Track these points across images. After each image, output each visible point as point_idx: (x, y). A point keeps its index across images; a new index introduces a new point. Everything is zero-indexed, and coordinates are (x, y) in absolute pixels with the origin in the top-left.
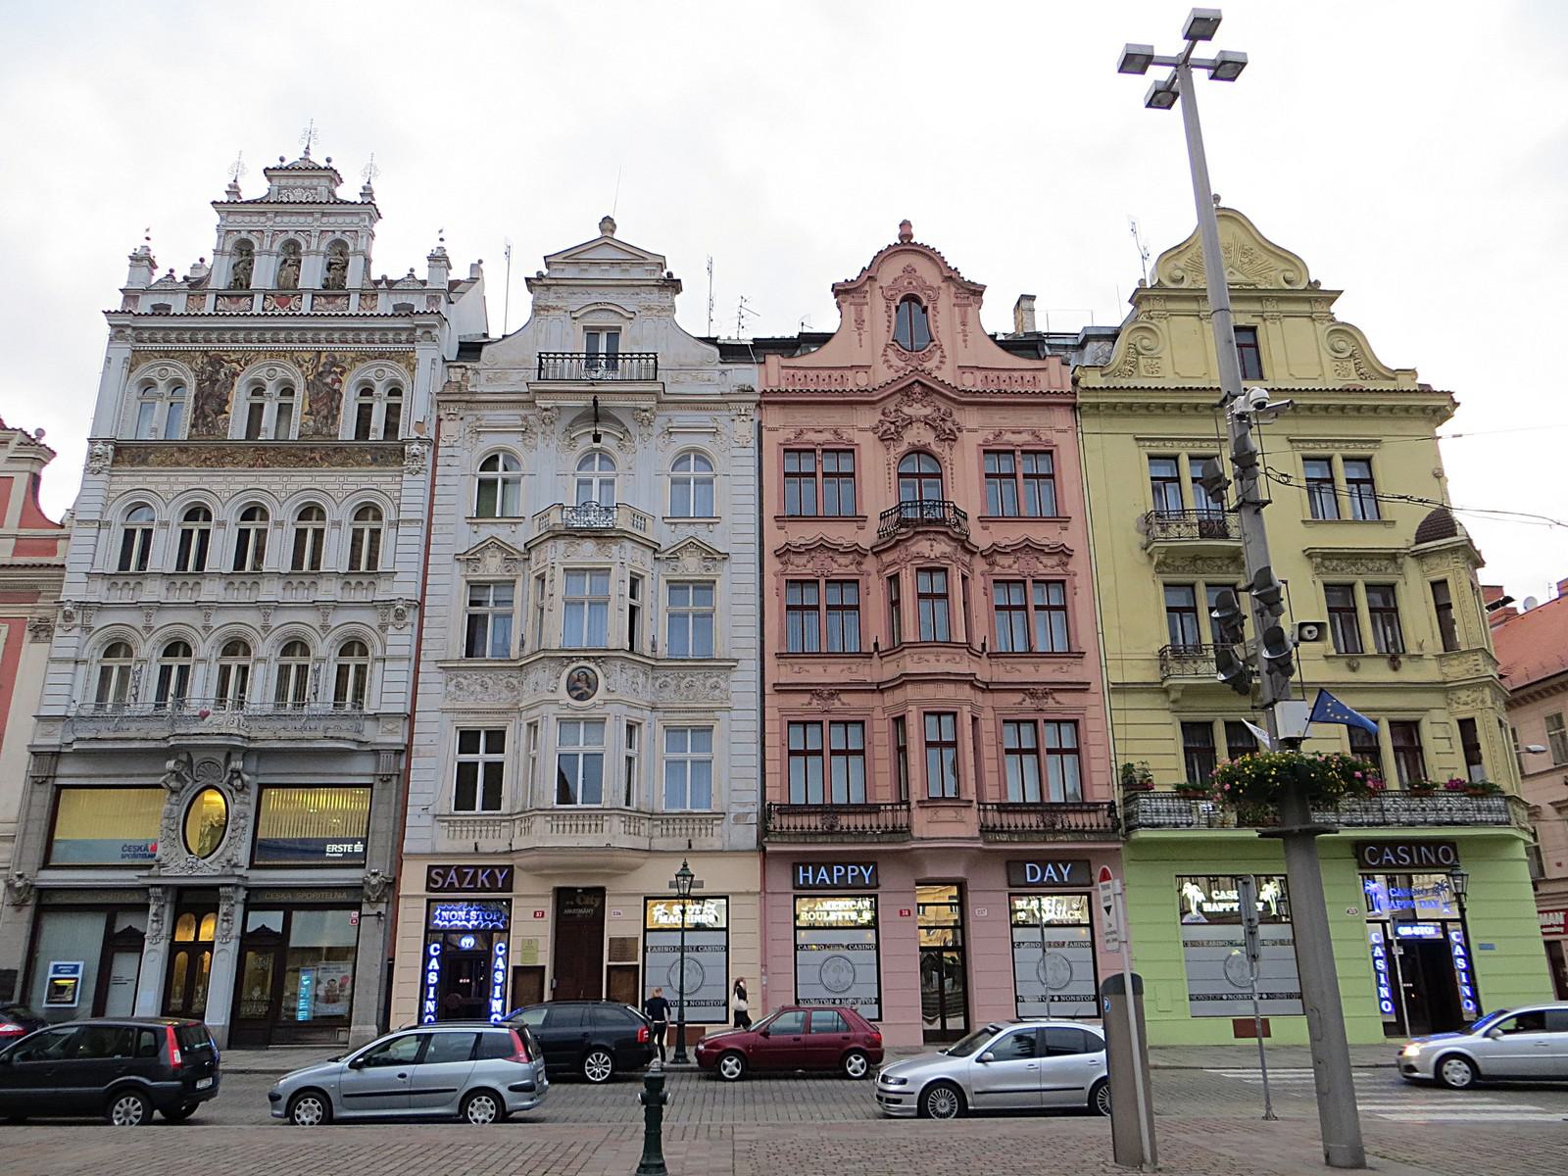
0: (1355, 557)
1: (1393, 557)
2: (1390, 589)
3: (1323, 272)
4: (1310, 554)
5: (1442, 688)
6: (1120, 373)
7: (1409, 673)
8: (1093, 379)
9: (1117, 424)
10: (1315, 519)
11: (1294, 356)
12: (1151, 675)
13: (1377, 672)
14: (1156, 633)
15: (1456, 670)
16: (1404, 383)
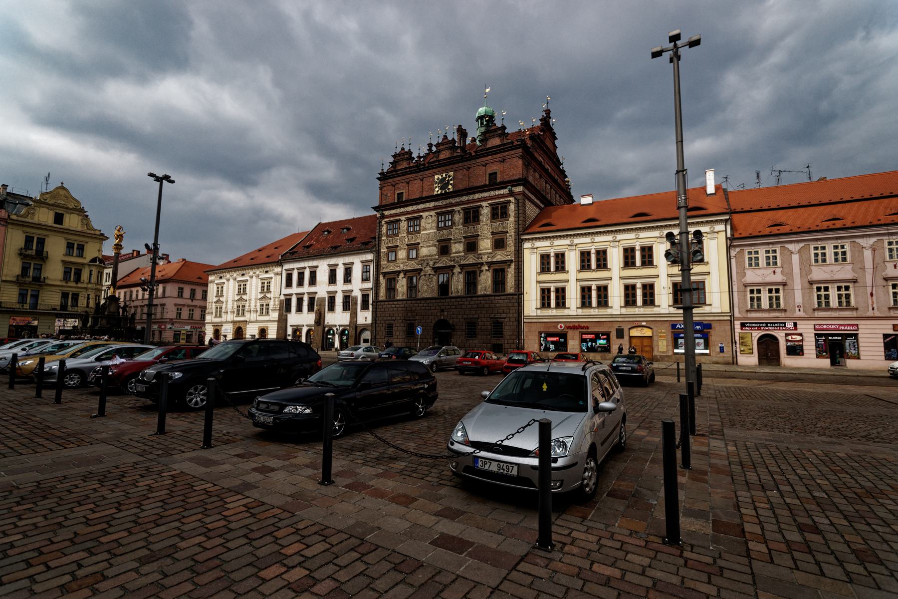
0: (73, 263)
1: (83, 264)
2: (81, 270)
3: (85, 205)
4: (63, 261)
5: (86, 289)
6: (21, 216)
7: (80, 285)
8: (14, 217)
9: (18, 227)
10: (68, 254)
11: (72, 222)
12: (14, 279)
13: (74, 284)
14: (17, 270)
15: (90, 286)
16: (98, 233)
